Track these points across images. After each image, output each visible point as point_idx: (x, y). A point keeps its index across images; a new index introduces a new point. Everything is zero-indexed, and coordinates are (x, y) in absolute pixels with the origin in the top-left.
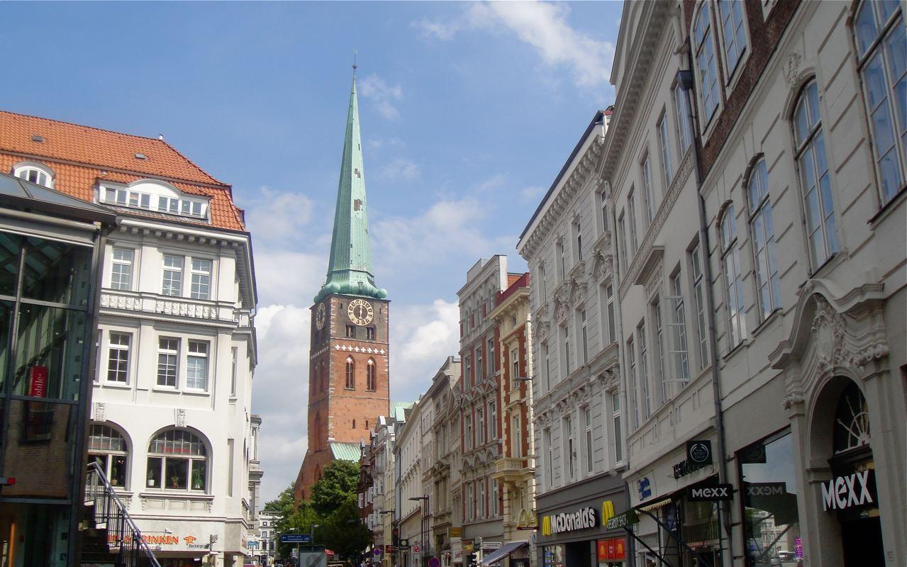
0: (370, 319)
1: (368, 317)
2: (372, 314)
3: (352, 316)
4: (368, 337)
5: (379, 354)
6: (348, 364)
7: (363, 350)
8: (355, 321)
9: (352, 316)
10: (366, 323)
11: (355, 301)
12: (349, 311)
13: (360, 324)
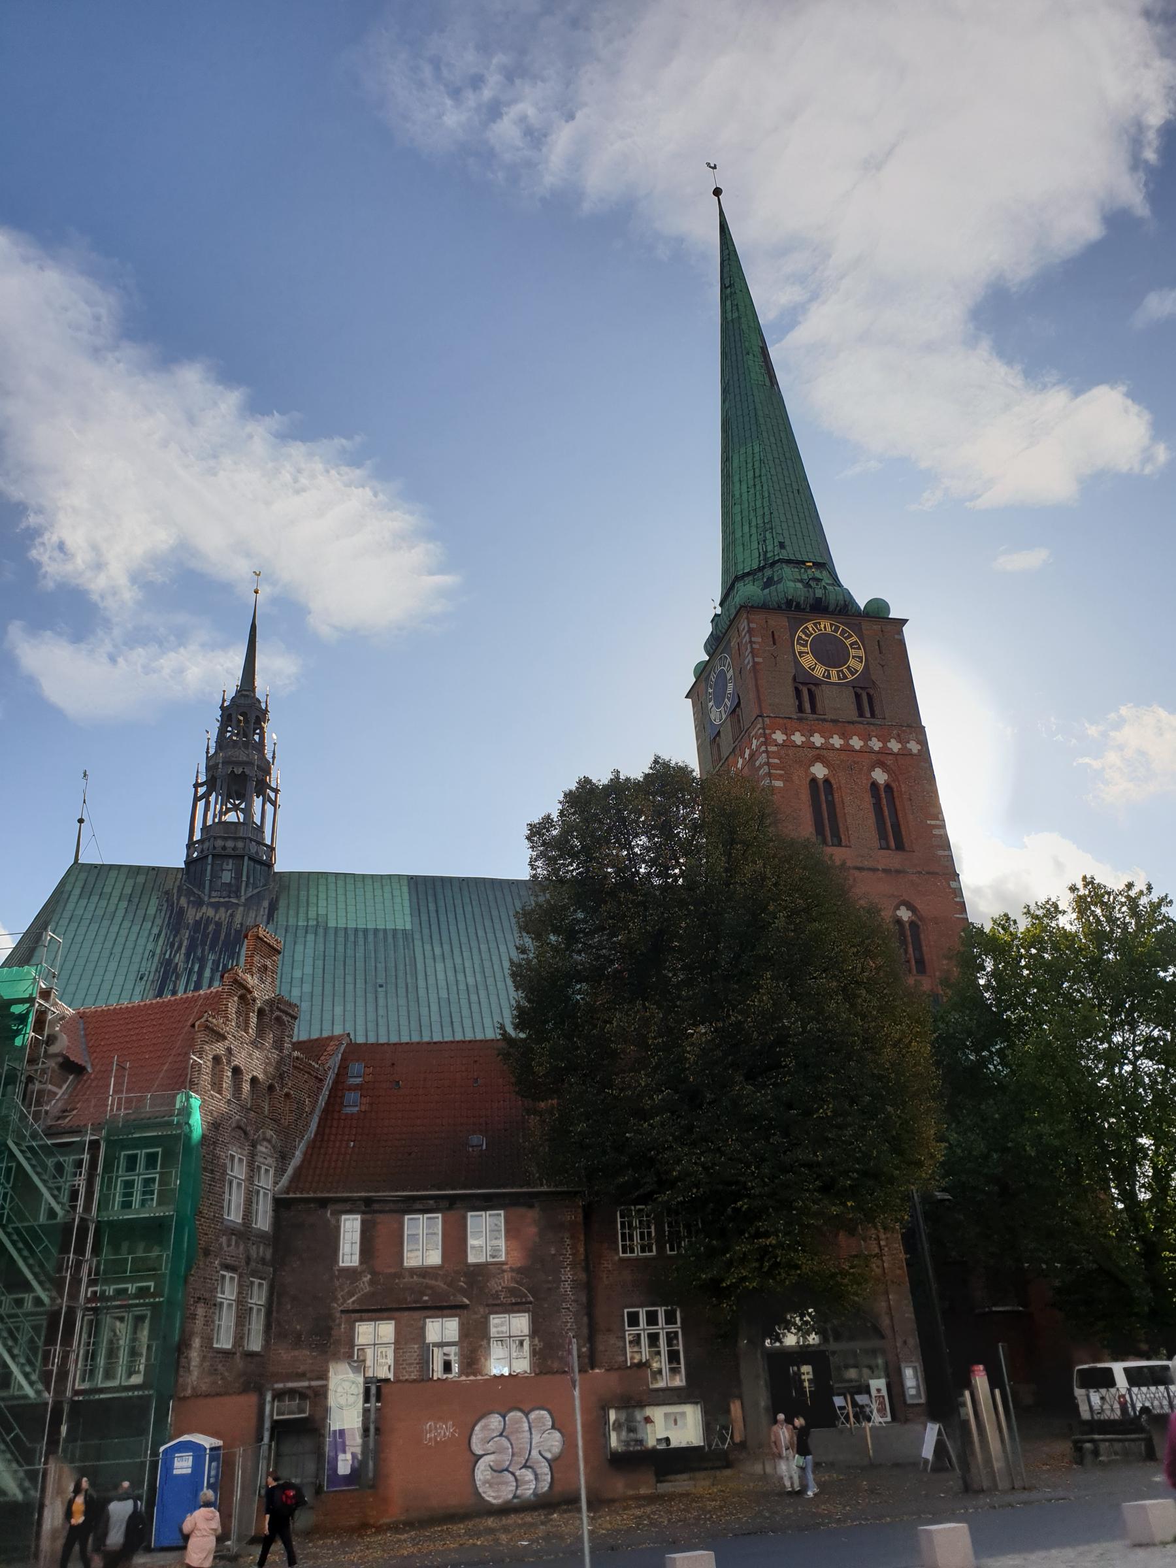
0: (860, 667)
1: (851, 662)
2: (862, 653)
3: (808, 661)
4: (861, 715)
5: (905, 753)
6: (814, 780)
7: (856, 743)
8: (819, 671)
9: (808, 661)
10: (850, 678)
11: (810, 625)
12: (798, 648)
13: (834, 679)
